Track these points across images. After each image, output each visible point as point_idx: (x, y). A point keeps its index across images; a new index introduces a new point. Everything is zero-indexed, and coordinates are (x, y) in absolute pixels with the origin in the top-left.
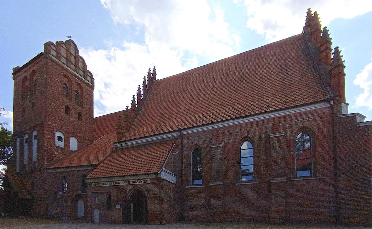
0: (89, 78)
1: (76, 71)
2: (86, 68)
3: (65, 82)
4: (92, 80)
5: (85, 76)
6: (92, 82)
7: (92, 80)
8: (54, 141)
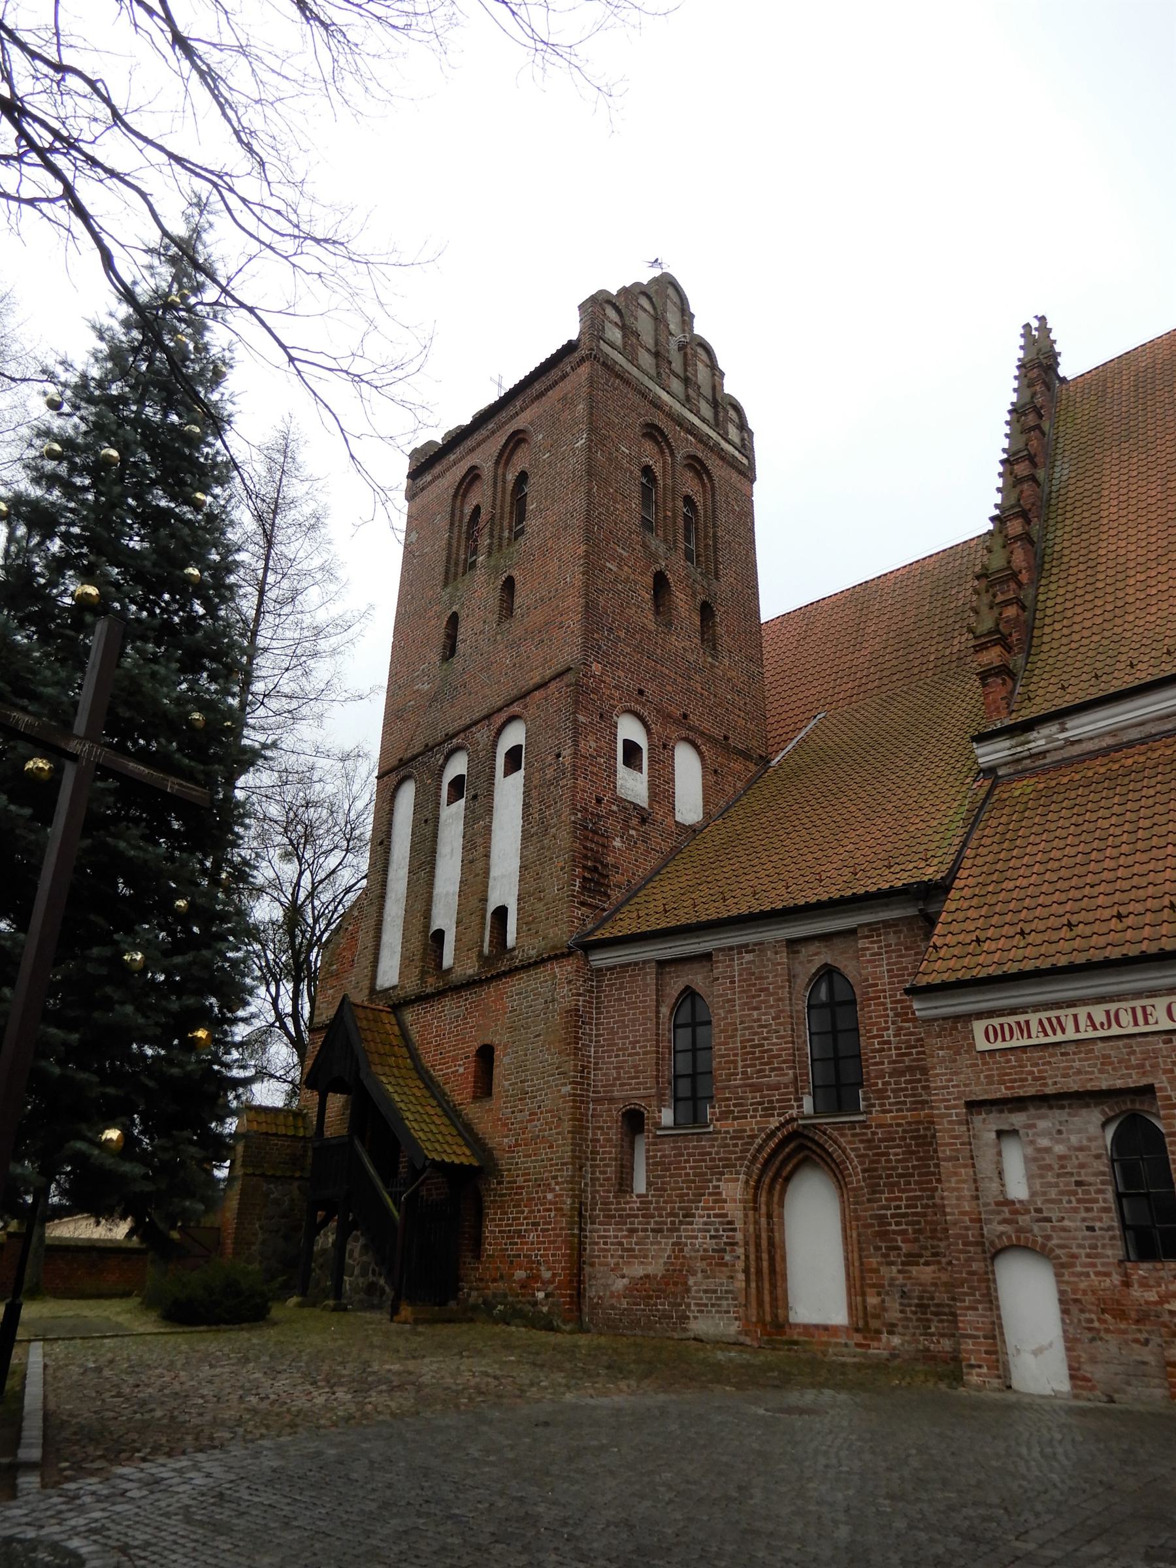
0: (733, 433)
1: (687, 401)
2: (722, 385)
4: (743, 440)
5: (718, 425)
6: (744, 446)
7: (746, 436)
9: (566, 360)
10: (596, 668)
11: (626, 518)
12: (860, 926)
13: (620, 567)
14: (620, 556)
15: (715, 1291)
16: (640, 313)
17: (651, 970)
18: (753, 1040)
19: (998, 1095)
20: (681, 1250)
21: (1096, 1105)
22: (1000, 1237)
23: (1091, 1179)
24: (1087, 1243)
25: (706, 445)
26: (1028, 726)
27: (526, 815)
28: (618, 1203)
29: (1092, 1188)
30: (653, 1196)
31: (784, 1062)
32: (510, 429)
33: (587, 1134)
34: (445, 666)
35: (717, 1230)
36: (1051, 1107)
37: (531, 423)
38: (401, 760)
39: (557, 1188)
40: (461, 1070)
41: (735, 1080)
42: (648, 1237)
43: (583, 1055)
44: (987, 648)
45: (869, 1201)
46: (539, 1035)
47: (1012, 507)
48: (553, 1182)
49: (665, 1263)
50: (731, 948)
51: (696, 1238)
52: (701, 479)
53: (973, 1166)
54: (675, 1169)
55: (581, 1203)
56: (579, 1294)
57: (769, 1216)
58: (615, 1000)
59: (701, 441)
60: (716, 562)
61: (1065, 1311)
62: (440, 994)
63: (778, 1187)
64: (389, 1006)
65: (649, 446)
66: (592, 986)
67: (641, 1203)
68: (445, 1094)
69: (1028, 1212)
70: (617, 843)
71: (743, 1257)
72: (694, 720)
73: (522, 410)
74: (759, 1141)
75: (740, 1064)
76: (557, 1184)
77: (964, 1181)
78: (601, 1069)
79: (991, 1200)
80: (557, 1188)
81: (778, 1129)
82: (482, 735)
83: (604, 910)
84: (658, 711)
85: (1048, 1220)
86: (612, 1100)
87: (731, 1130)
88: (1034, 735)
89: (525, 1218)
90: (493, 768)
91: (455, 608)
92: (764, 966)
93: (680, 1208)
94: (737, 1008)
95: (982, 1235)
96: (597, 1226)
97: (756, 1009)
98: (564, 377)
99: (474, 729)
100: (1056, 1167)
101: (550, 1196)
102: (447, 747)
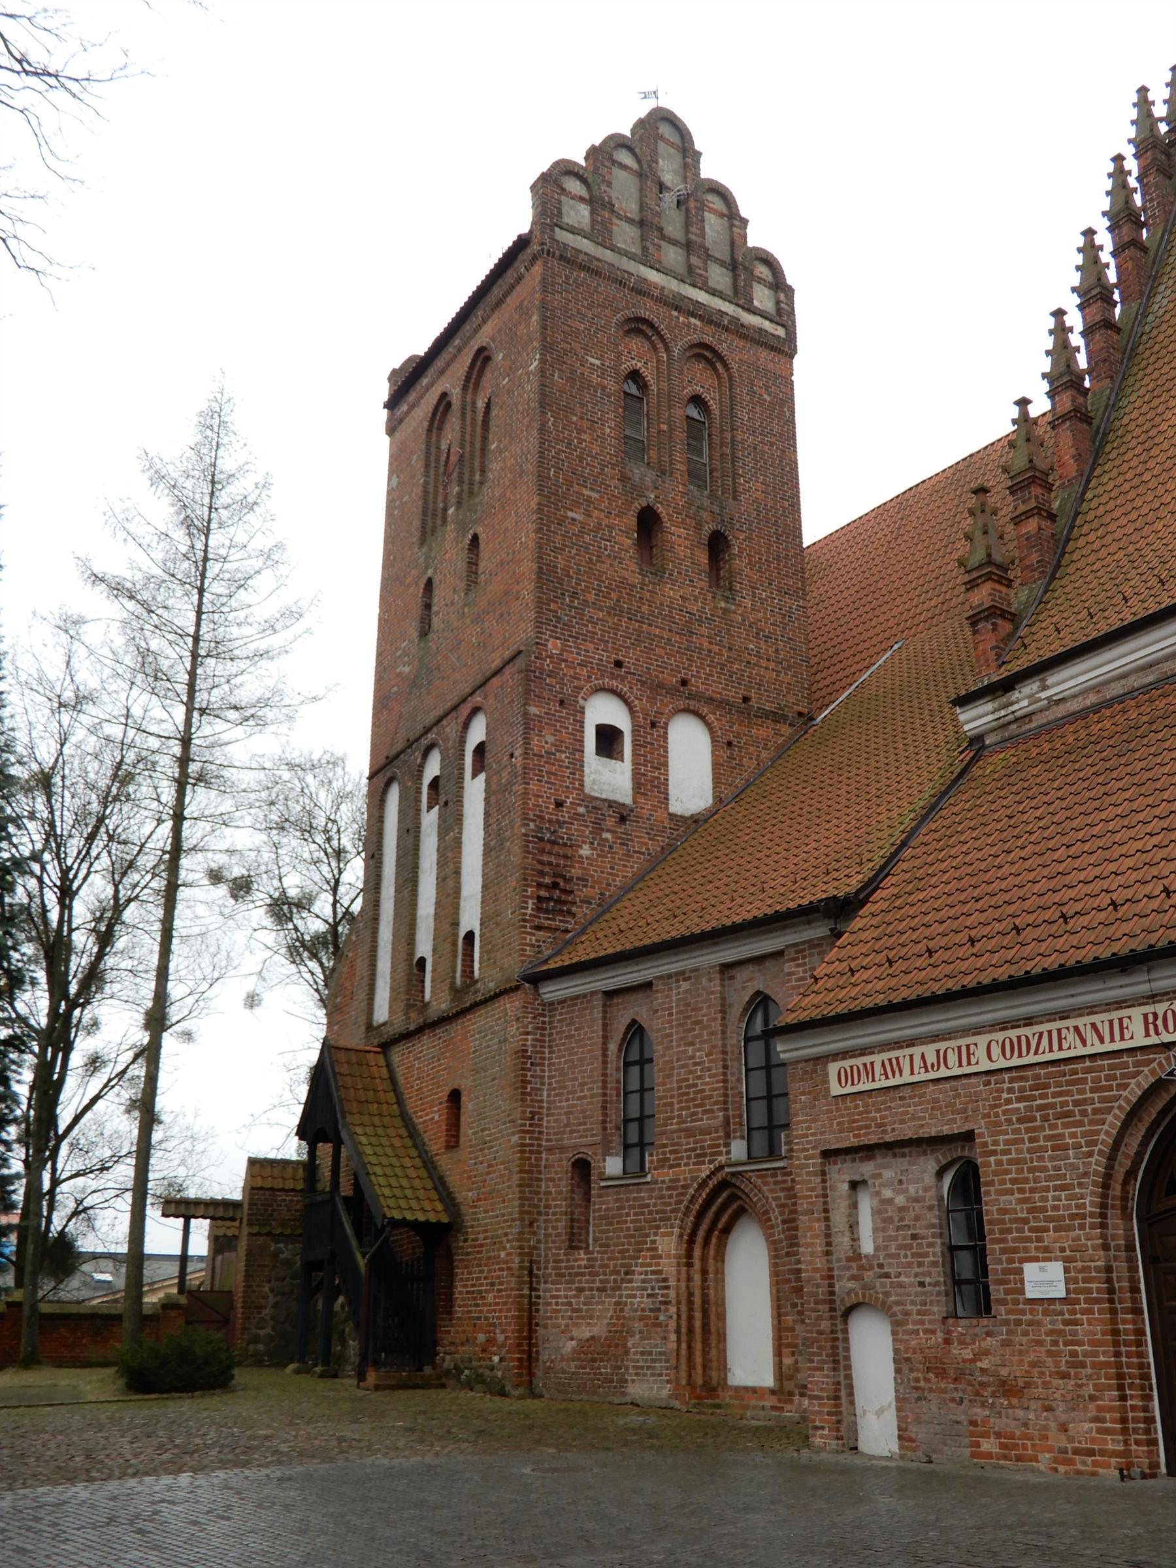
2: (745, 237)
3: (634, 362)
7: (782, 296)
8: (578, 766)
9: (521, 257)
10: (554, 646)
11: (596, 449)
12: (787, 946)
13: (588, 514)
14: (589, 500)
15: (650, 1353)
16: (616, 171)
17: (598, 1002)
18: (688, 1080)
19: (847, 1144)
20: (622, 1310)
21: (932, 1152)
22: (848, 1294)
23: (923, 1232)
24: (918, 1299)
25: (717, 325)
26: (1007, 685)
27: (487, 826)
28: (568, 1261)
29: (924, 1242)
30: (598, 1252)
31: (716, 1103)
32: (475, 345)
33: (540, 1187)
34: (422, 645)
35: (653, 1288)
36: (895, 1155)
37: (493, 339)
38: (387, 757)
39: (508, 1246)
40: (437, 1118)
41: (672, 1124)
42: (593, 1297)
43: (532, 1100)
44: (978, 585)
45: (788, 1255)
46: (494, 1079)
47: (1061, 376)
48: (504, 1239)
49: (608, 1324)
50: (670, 976)
51: (634, 1296)
52: (715, 369)
53: (827, 1219)
54: (618, 1223)
55: (531, 1262)
56: (530, 1357)
57: (704, 1272)
58: (566, 1037)
59: (710, 322)
60: (735, 475)
61: (898, 1371)
62: (420, 1030)
63: (714, 1240)
64: (378, 1046)
65: (636, 344)
66: (544, 1022)
67: (588, 1260)
68: (424, 1144)
69: (871, 1267)
70: (585, 851)
71: (675, 1317)
72: (697, 685)
73: (484, 321)
74: (691, 1191)
75: (676, 1106)
76: (508, 1241)
77: (817, 1236)
78: (553, 1115)
79: (843, 1256)
80: (508, 1246)
81: (709, 1177)
82: (451, 728)
83: (567, 931)
84: (643, 683)
85: (887, 1276)
86: (562, 1149)
87: (667, 1179)
88: (1015, 695)
89: (485, 1278)
90: (461, 769)
91: (430, 572)
92: (699, 996)
93: (622, 1266)
94: (674, 1044)
95: (832, 1293)
96: (549, 1286)
97: (692, 1044)
98: (520, 279)
99: (444, 722)
100: (896, 1219)
101: (503, 1254)
102: (425, 742)
